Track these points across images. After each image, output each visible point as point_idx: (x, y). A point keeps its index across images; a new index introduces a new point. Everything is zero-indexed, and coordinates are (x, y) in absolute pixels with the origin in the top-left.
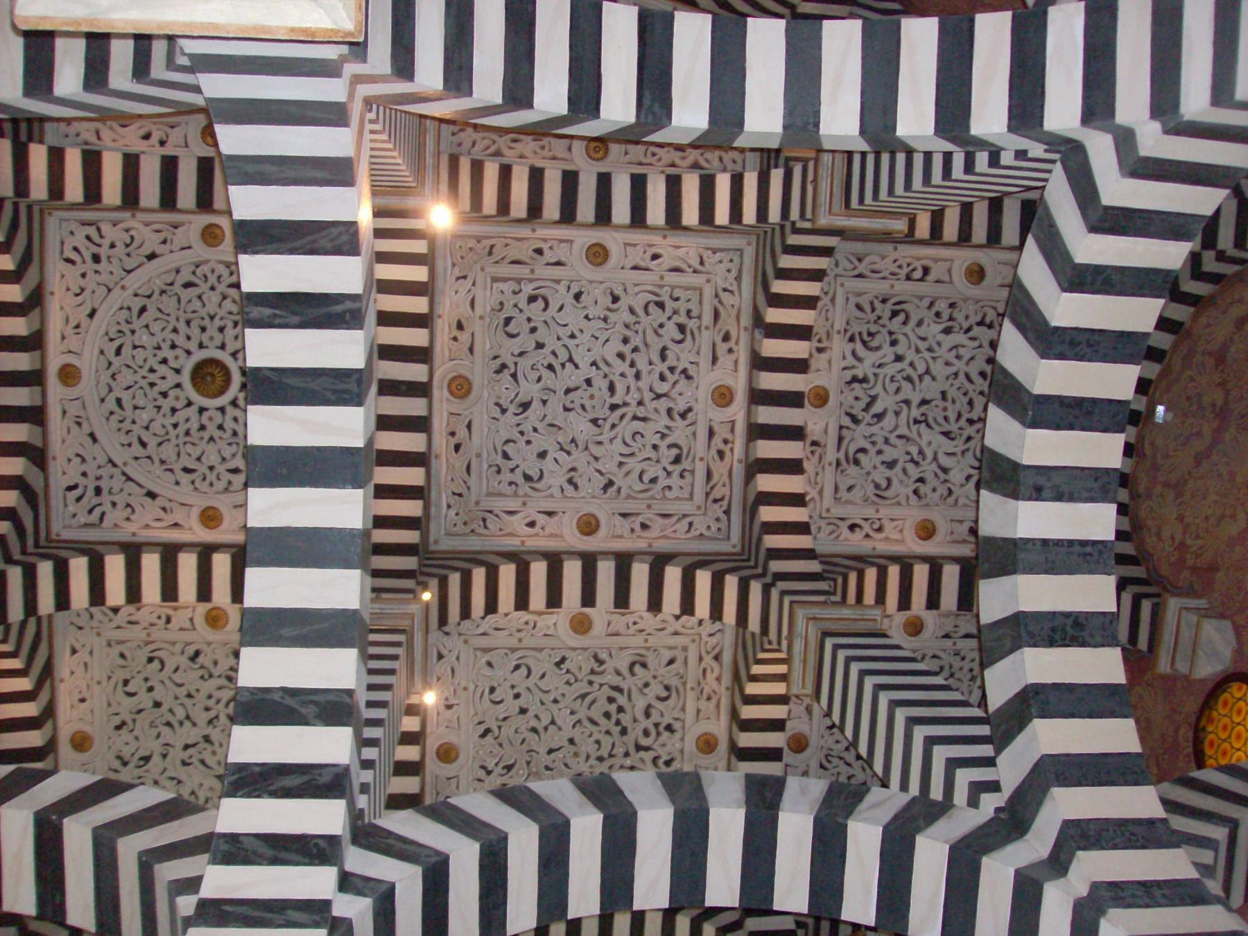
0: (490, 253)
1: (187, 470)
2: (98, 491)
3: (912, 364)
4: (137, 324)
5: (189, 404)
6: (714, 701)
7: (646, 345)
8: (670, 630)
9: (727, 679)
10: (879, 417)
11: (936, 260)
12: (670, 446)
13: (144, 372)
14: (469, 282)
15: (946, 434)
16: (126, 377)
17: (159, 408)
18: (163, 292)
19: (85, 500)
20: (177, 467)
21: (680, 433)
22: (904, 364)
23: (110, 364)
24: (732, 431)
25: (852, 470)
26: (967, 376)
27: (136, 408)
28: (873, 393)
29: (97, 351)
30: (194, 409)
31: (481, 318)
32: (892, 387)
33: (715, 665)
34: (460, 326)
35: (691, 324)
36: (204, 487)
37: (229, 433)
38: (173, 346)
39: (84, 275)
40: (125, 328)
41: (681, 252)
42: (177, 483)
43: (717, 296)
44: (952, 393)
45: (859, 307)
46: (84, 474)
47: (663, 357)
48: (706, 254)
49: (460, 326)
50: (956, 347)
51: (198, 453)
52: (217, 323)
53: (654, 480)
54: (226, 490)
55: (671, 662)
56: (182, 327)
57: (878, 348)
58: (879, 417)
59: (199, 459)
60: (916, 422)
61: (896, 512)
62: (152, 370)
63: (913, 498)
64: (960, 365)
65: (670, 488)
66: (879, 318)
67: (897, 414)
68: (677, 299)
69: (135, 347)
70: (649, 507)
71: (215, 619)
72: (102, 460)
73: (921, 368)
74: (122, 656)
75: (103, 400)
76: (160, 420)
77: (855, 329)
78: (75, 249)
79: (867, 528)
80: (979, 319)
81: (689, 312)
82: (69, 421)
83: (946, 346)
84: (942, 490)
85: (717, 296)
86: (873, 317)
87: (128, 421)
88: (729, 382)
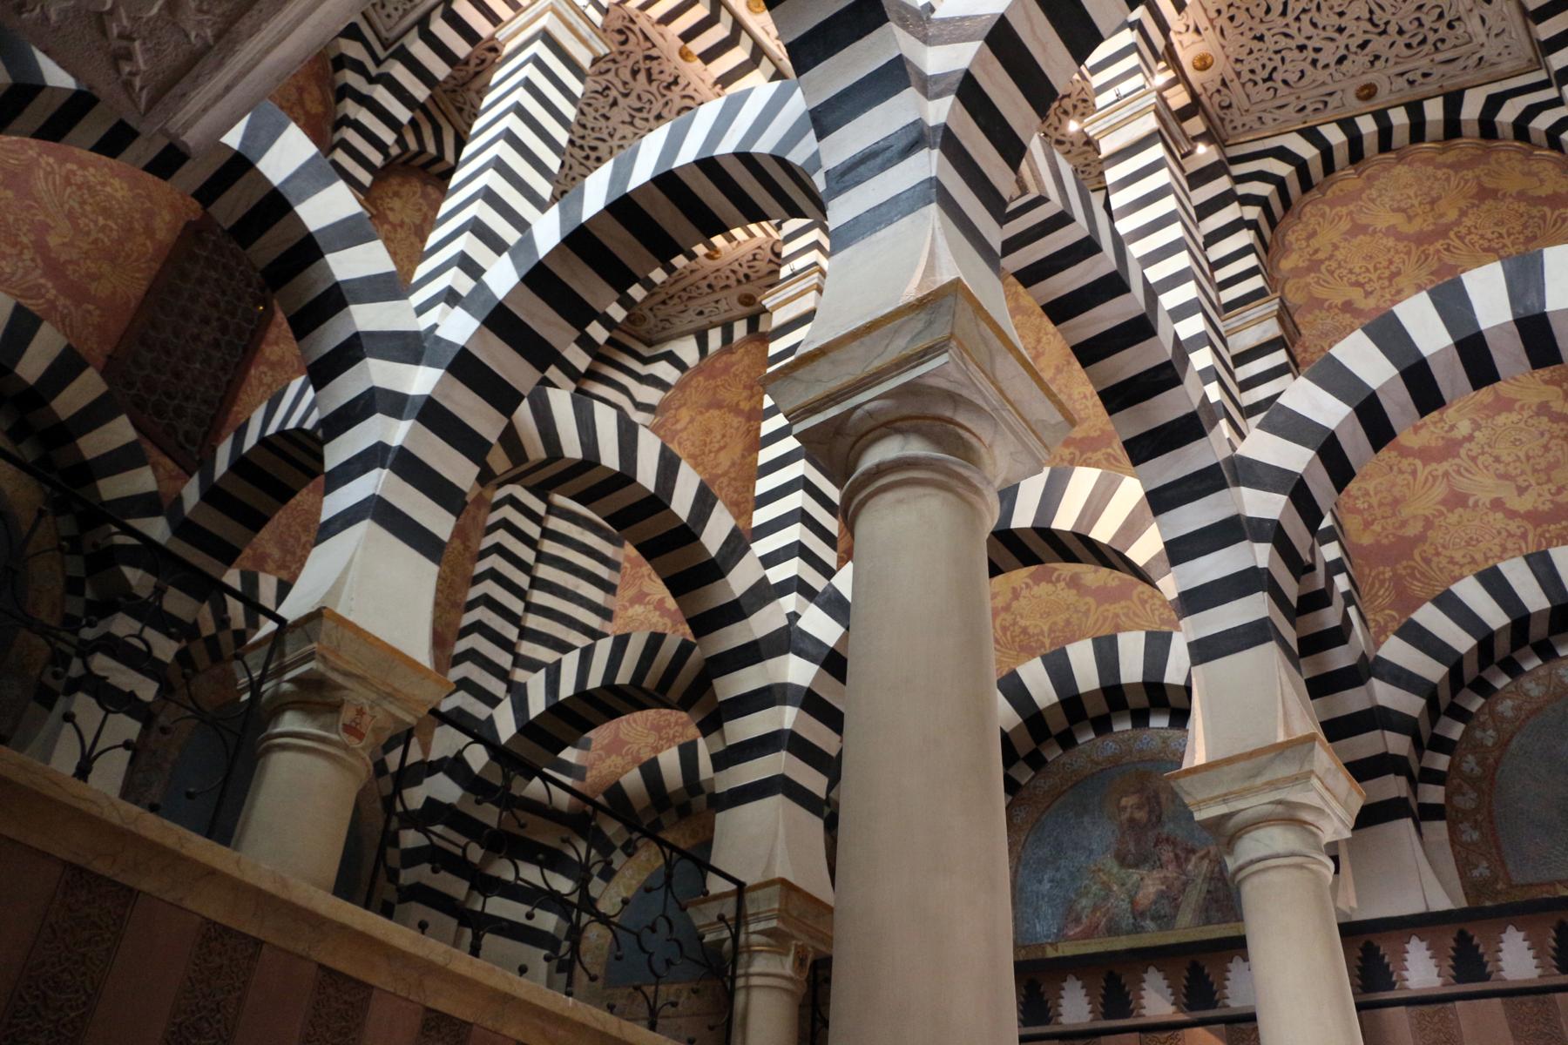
3: (647, 120)
10: (635, 73)
22: (651, 116)
25: (618, 25)
28: (655, 84)
32: (645, 97)
44: (602, 123)
58: (635, 73)
67: (625, 83)
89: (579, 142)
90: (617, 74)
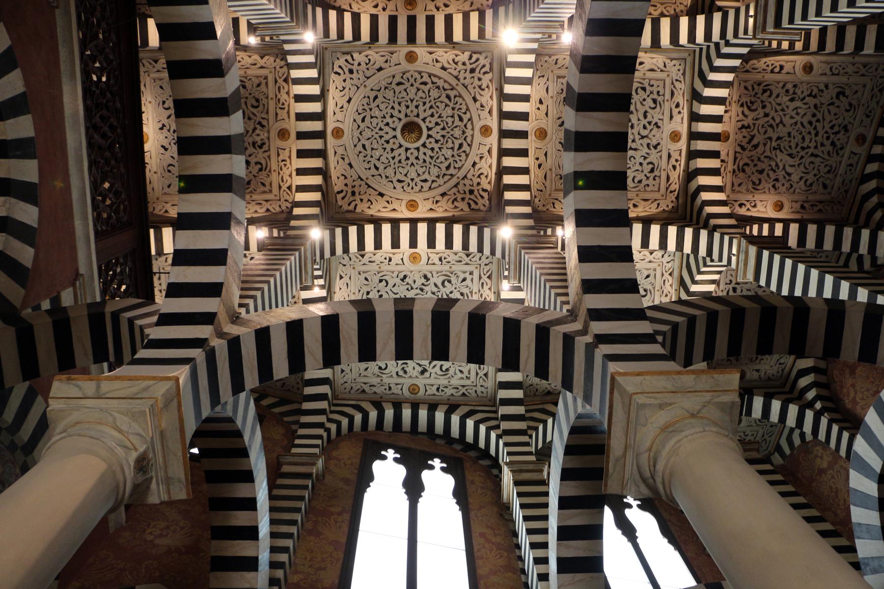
0: (556, 63)
1: (399, 181)
2: (353, 193)
3: (773, 118)
4: (373, 105)
5: (401, 146)
6: (669, 297)
7: (637, 110)
8: (647, 260)
9: (675, 286)
10: (756, 147)
11: (787, 62)
12: (648, 164)
13: (377, 130)
14: (545, 79)
15: (790, 155)
16: (368, 133)
17: (385, 149)
18: (386, 88)
19: (347, 198)
20: (394, 180)
21: (653, 157)
23: (359, 126)
24: (680, 155)
25: (741, 175)
26: (802, 124)
27: (372, 149)
28: (752, 134)
29: (352, 120)
30: (403, 149)
31: (552, 97)
32: (762, 131)
33: (670, 278)
34: (541, 102)
35: (660, 99)
36: (409, 189)
37: (422, 161)
38: (392, 116)
39: (345, 81)
40: (366, 107)
41: (654, 61)
42: (395, 188)
43: (672, 83)
44: (794, 133)
45: (746, 88)
46: (346, 185)
47: (645, 117)
48: (668, 61)
49: (541, 102)
50: (796, 108)
51: (405, 172)
52: (415, 103)
53: (640, 182)
54: (420, 191)
55: (648, 276)
56: (396, 106)
57: (756, 110)
58: (756, 147)
59: (406, 175)
60: (775, 149)
61: (763, 197)
62: (381, 129)
63: (772, 190)
64: (798, 118)
65: (648, 185)
66: (756, 94)
67: (765, 145)
68: (652, 86)
69: (372, 117)
70: (637, 195)
71: (415, 258)
72: (355, 177)
73: (778, 120)
74: (366, 279)
75: (355, 146)
76: (385, 155)
77: (744, 100)
78: (340, 67)
79: (748, 206)
80: (809, 92)
81: (658, 92)
82: (338, 157)
83: (791, 108)
84: (787, 185)
85: (672, 83)
86: (753, 93)
87: (369, 156)
88: (679, 129)
89: (813, 132)
90: (764, 152)
